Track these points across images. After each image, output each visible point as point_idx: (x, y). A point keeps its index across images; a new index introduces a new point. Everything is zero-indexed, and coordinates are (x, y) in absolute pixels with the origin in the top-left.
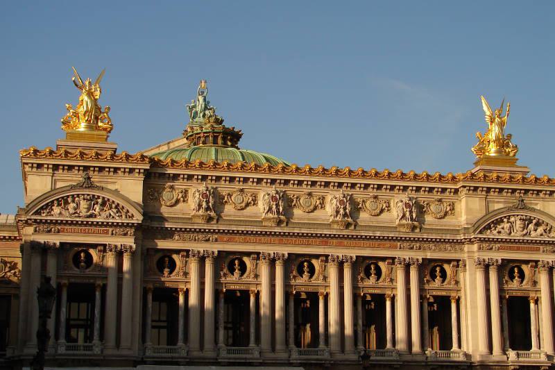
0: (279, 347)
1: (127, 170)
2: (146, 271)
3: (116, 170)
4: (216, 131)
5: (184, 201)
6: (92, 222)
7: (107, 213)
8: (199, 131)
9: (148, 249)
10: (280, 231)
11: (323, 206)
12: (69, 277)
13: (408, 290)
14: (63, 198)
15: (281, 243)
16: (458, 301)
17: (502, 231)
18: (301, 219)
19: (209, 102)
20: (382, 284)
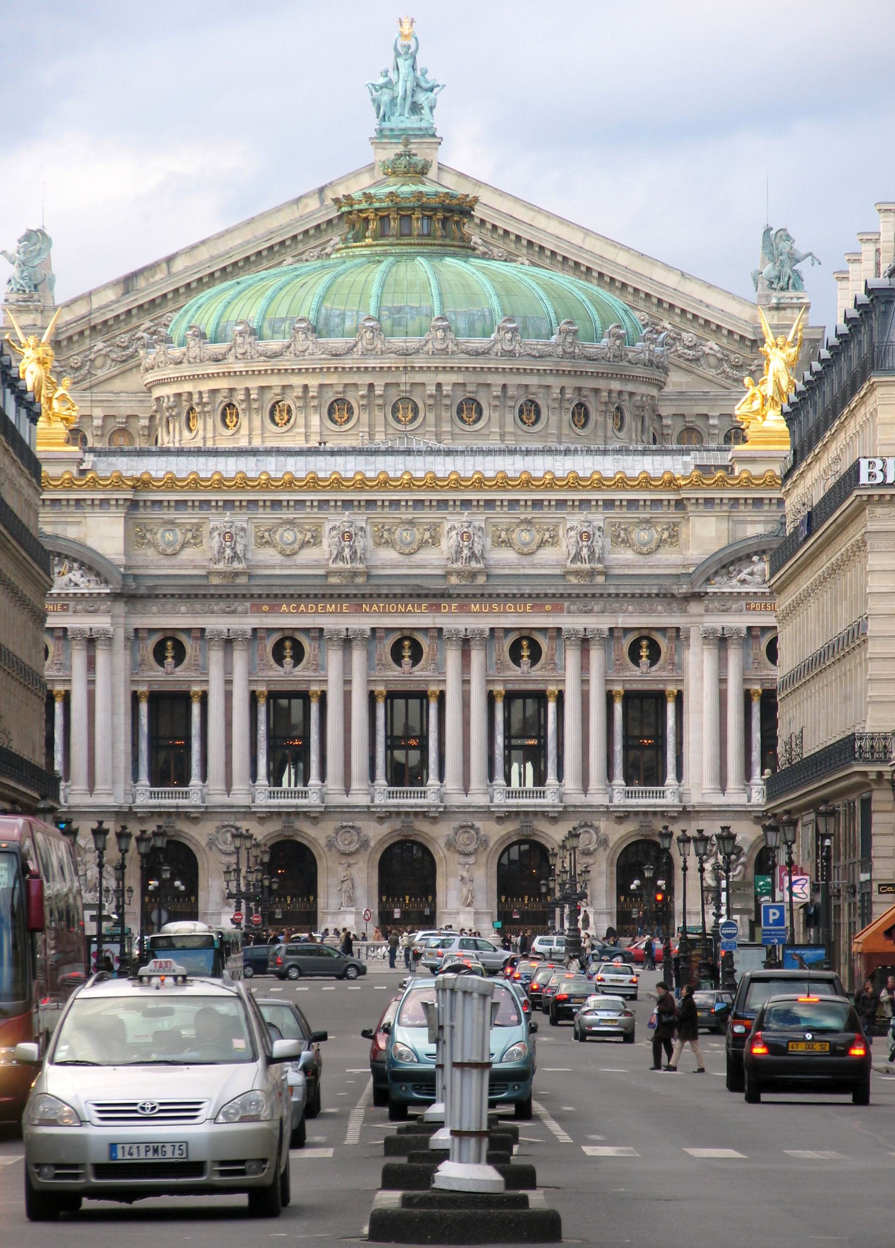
0: (355, 785)
1: (97, 502)
2: (136, 666)
3: (78, 501)
4: (403, 204)
5: (195, 544)
8: (364, 206)
9: (136, 630)
10: (354, 592)
11: (435, 541)
13: (585, 682)
15: (358, 610)
16: (679, 698)
17: (749, 578)
18: (396, 567)
19: (424, 72)
20: (539, 673)
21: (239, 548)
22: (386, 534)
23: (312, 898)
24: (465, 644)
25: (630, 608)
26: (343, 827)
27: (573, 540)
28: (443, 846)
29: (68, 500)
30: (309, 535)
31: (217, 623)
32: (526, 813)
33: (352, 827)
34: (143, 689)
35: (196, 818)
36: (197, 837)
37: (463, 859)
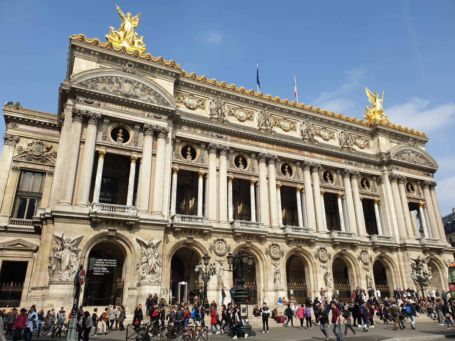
6: (133, 102)
7: (146, 98)
10: (273, 138)
12: (107, 147)
14: (107, 77)
21: (223, 111)
22: (278, 122)
23: (254, 283)
24: (312, 169)
25: (364, 165)
26: (273, 245)
27: (344, 137)
28: (314, 257)
29: (148, 66)
30: (249, 115)
31: (215, 141)
32: (344, 243)
33: (277, 245)
34: (177, 167)
35: (205, 234)
36: (204, 245)
37: (323, 264)
